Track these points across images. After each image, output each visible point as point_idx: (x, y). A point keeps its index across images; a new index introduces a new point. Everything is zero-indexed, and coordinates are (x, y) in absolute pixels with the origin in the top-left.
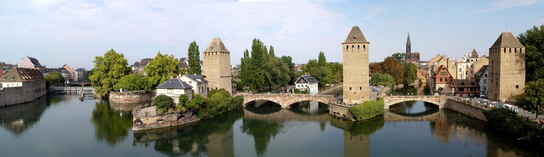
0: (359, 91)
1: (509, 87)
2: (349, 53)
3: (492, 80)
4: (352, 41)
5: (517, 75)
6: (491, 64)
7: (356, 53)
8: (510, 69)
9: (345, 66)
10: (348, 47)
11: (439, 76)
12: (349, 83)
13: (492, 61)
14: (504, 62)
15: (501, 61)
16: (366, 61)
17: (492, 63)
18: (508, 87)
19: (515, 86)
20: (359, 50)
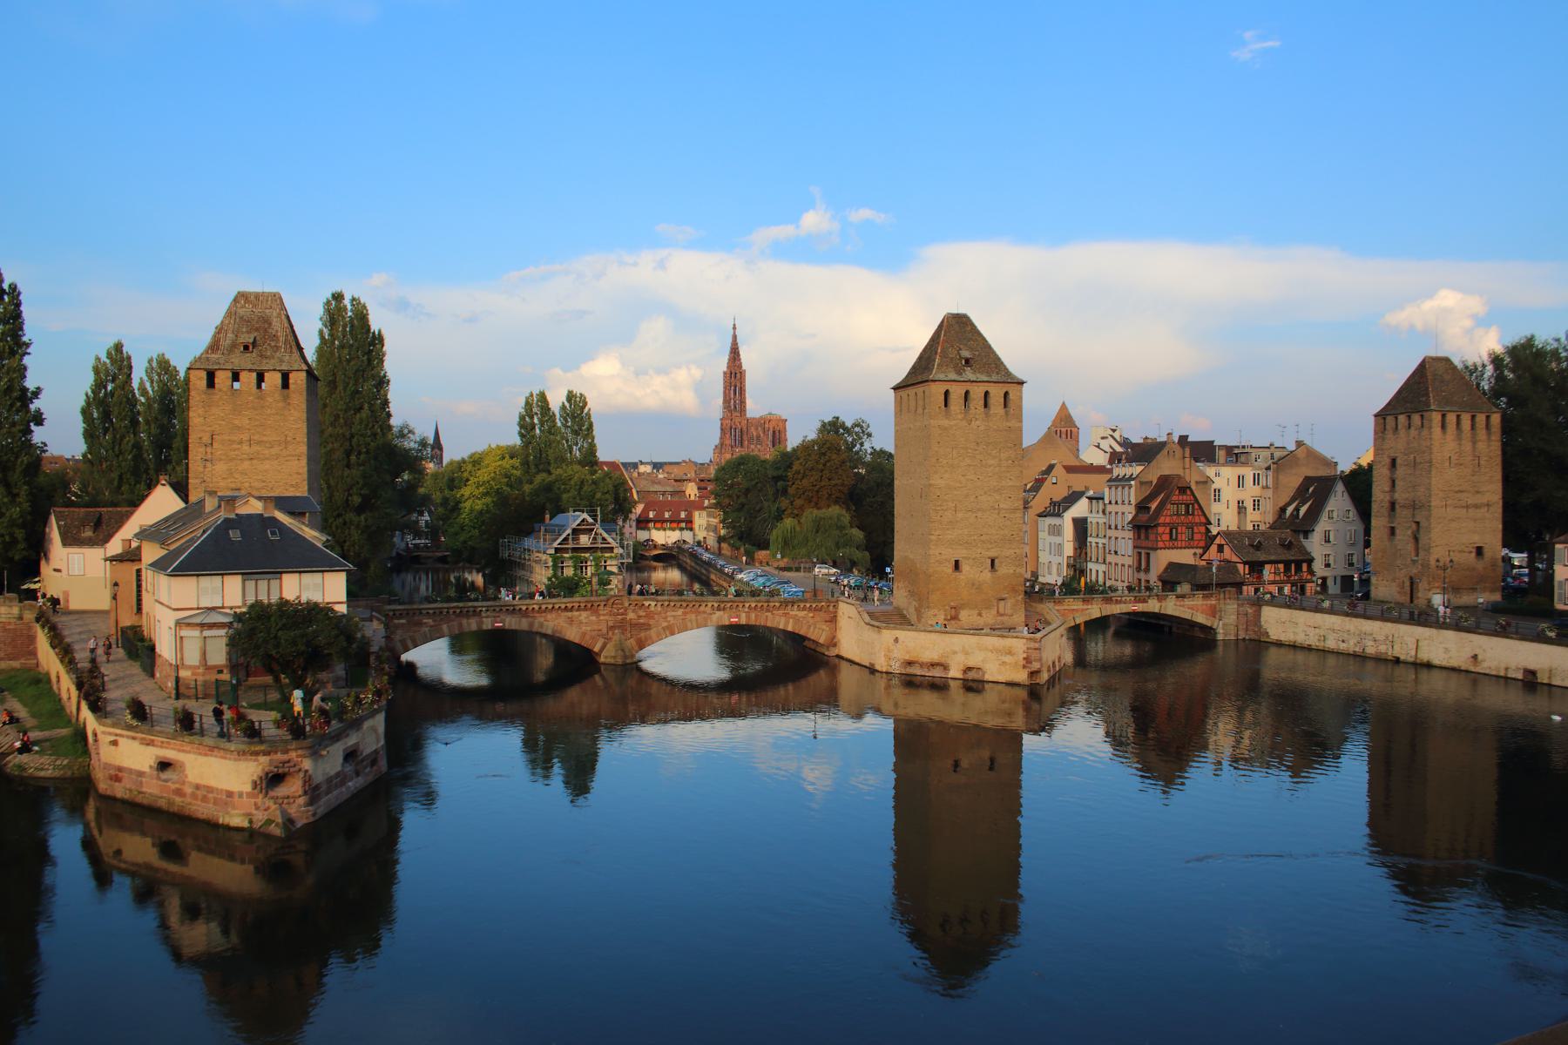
0: (987, 575)
2: (952, 423)
5: (1478, 511)
7: (978, 422)
8: (1460, 488)
10: (947, 393)
11: (1168, 520)
13: (1387, 461)
18: (1454, 551)
19: (1474, 550)
20: (987, 415)
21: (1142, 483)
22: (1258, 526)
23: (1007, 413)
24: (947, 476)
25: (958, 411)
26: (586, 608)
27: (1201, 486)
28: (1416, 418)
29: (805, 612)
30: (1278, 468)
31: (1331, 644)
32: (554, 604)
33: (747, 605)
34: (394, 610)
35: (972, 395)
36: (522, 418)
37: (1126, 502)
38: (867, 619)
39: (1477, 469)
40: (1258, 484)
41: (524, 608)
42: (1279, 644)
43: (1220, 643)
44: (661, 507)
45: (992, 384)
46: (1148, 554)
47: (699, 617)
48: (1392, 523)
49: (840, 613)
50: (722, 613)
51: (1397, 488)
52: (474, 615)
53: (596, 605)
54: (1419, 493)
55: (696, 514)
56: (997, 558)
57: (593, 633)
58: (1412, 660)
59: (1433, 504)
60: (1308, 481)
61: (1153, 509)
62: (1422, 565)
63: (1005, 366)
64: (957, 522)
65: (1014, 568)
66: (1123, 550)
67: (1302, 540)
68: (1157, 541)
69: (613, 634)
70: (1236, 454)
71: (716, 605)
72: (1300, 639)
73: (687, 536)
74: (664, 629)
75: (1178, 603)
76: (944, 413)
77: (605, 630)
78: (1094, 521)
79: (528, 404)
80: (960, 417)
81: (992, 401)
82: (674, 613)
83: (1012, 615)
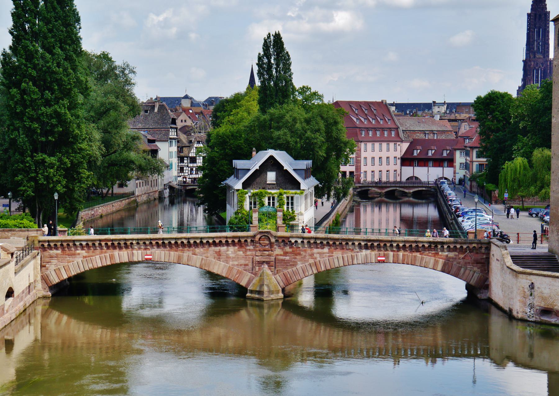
26: (234, 244)
29: (457, 254)
32: (201, 238)
33: (395, 245)
34: (49, 241)
36: (260, 59)
38: (509, 261)
41: (173, 242)
44: (426, 144)
47: (345, 255)
49: (492, 253)
50: (369, 252)
52: (126, 247)
53: (243, 240)
55: (458, 153)
57: (241, 269)
69: (259, 269)
71: (363, 243)
73: (448, 172)
74: (310, 265)
77: (250, 266)
79: (266, 46)
82: (320, 250)
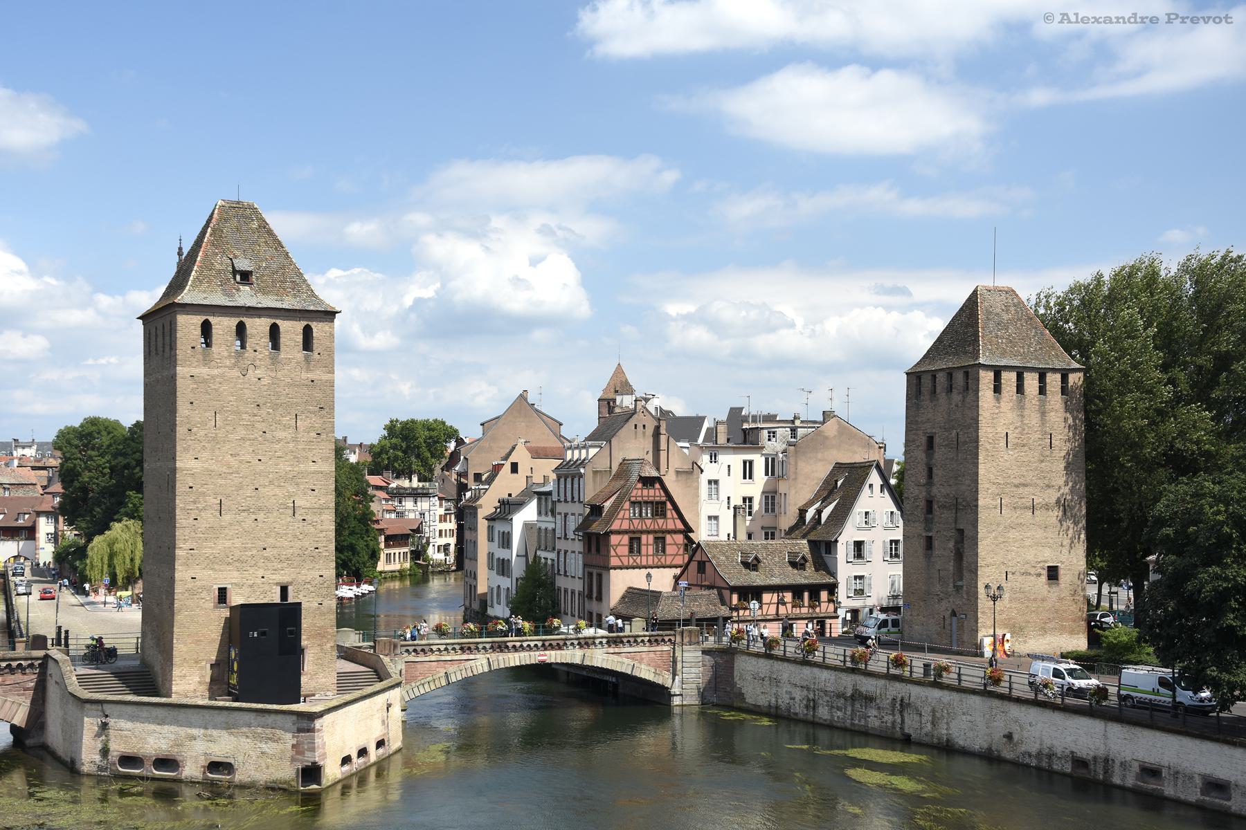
1: (1020, 578)
2: (215, 372)
3: (929, 540)
4: (230, 295)
6: (920, 455)
8: (1022, 481)
9: (186, 450)
11: (625, 526)
12: (212, 562)
13: (924, 439)
14: (995, 441)
15: (982, 440)
16: (317, 422)
17: (924, 447)
18: (1013, 574)
19: (1045, 572)
20: (274, 361)
21: (595, 473)
22: (773, 534)
23: (307, 359)
24: (204, 455)
25: (226, 354)
27: (684, 477)
28: (959, 378)
30: (796, 451)
31: (823, 713)
35: (249, 330)
37: (576, 499)
39: (1048, 453)
40: (773, 474)
42: (756, 711)
43: (677, 710)
45: (283, 313)
46: (600, 576)
48: (930, 530)
49: (49, 672)
51: (936, 479)
54: (963, 488)
56: (291, 583)
58: (927, 739)
59: (981, 503)
60: (839, 467)
61: (606, 510)
62: (968, 593)
63: (308, 286)
64: (223, 528)
65: (319, 600)
66: (573, 570)
67: (824, 555)
68: (608, 556)
70: (744, 431)
72: (784, 701)
75: (611, 650)
76: (201, 357)
78: (543, 527)
80: (228, 363)
81: (284, 339)
83: (315, 675)
